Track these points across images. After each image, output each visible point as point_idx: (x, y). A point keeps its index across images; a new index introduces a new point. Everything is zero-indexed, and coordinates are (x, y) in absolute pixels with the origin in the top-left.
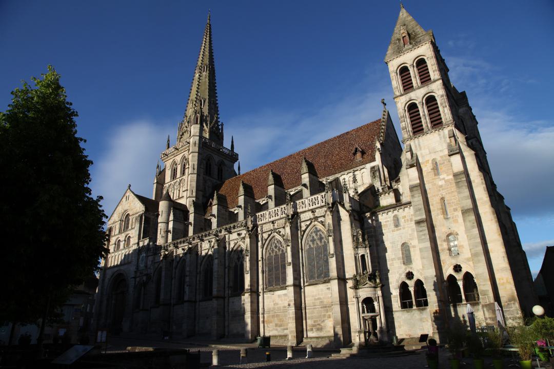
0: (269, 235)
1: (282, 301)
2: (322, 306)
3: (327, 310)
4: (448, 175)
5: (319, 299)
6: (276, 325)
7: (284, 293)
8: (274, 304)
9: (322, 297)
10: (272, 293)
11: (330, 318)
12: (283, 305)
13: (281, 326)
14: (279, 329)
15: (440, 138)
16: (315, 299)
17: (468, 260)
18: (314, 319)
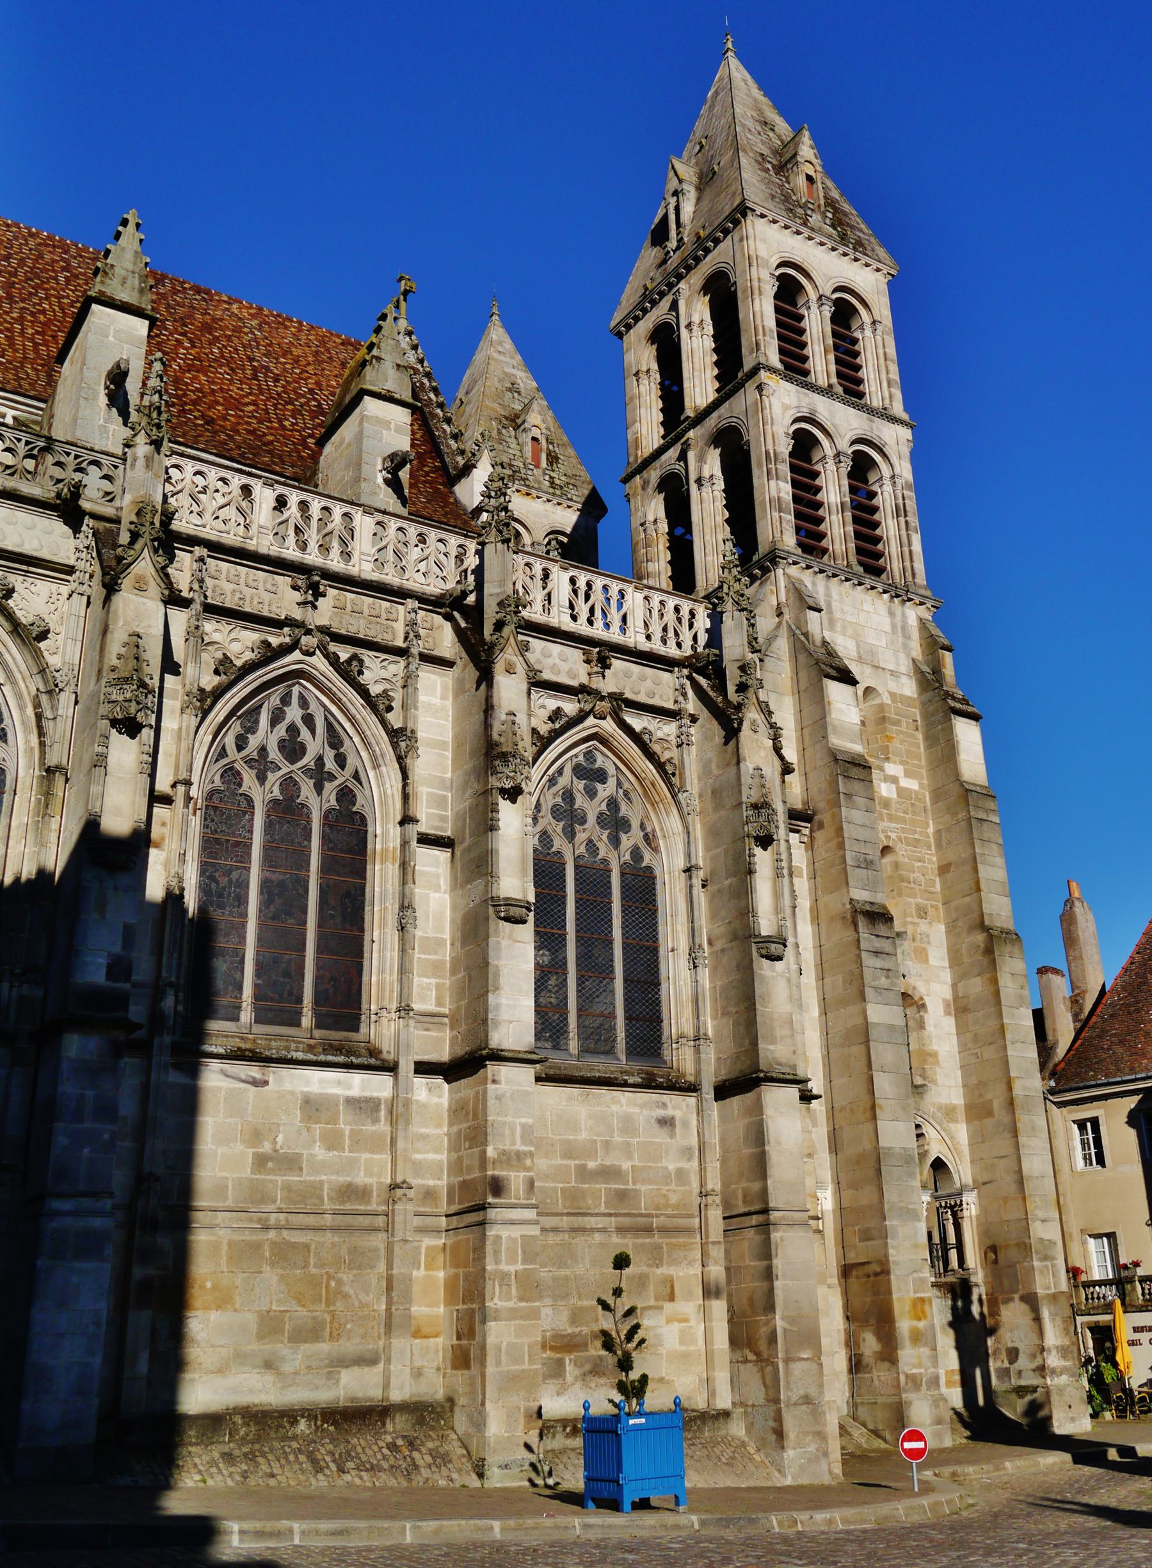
0: (271, 655)
1: (332, 1142)
2: (626, 1221)
3: (658, 1248)
4: (908, 774)
5: (609, 1173)
6: (270, 1326)
7: (355, 1092)
8: (261, 1161)
9: (626, 1165)
10: (253, 1071)
11: (672, 1298)
12: (342, 1179)
13: (310, 1333)
14: (294, 1357)
15: (894, 626)
16: (584, 1174)
17: (949, 1112)
18: (574, 1301)
